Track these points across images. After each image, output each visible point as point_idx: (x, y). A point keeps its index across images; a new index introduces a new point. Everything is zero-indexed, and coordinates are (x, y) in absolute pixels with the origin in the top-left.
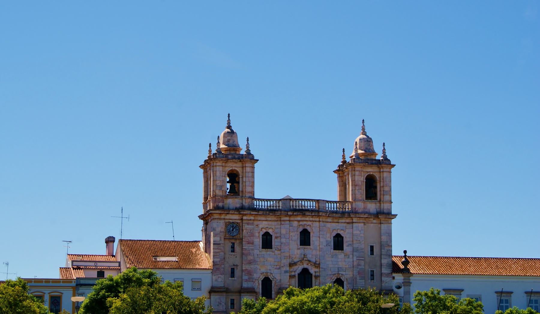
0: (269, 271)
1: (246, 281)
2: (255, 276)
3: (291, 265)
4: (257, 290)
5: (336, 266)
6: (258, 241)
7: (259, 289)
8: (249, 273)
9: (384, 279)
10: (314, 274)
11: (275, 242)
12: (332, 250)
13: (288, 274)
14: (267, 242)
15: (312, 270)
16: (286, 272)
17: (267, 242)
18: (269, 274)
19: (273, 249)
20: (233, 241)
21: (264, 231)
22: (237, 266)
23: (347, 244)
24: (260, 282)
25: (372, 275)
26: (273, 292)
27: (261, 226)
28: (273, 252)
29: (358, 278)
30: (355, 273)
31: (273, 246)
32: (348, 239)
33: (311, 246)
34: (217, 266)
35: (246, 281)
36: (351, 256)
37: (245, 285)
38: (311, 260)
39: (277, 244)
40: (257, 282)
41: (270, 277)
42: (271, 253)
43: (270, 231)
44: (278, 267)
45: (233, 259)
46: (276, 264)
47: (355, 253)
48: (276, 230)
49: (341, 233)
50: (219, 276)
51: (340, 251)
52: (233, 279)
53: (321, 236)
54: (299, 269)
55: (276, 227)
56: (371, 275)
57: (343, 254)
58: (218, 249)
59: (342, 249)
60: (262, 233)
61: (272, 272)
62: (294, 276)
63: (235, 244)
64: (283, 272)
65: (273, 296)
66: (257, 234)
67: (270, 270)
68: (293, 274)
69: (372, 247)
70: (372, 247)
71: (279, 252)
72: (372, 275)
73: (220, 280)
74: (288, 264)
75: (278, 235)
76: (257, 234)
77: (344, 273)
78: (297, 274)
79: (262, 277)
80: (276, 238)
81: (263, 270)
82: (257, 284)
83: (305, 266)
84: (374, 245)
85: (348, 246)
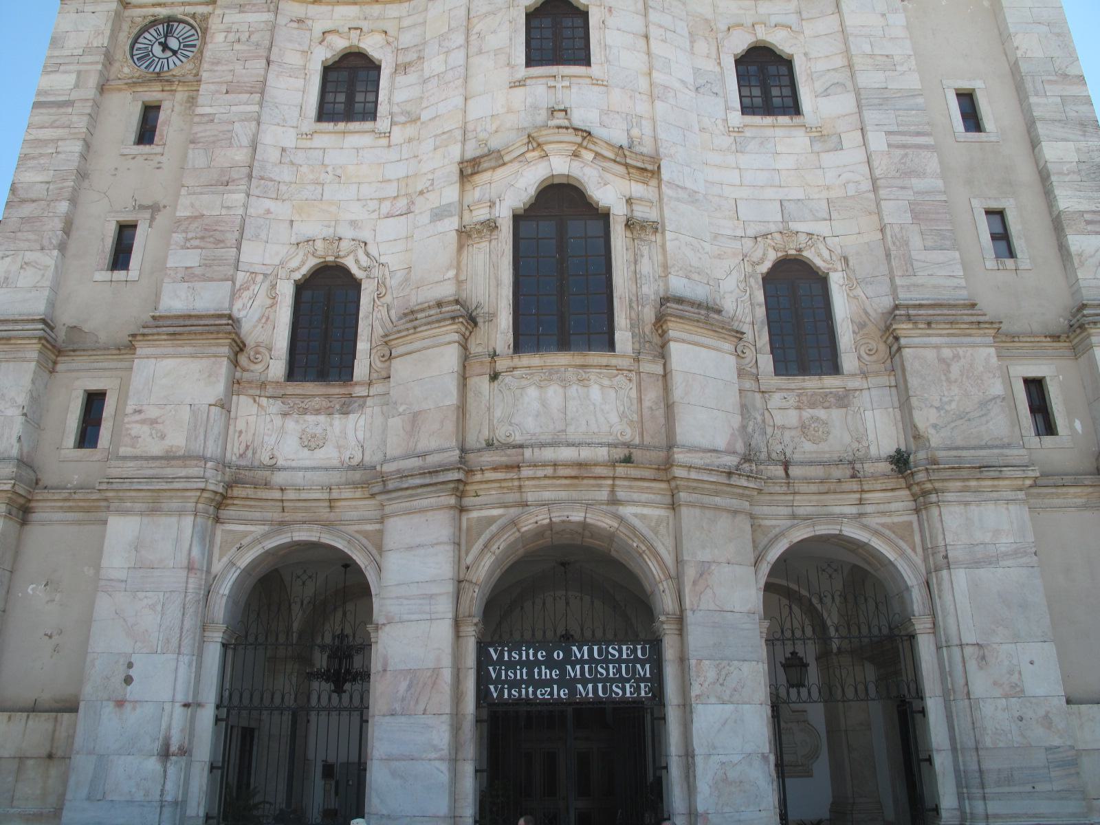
0: (347, 232)
1: (188, 276)
2: (252, 254)
3: (469, 170)
4: (251, 330)
5: (770, 193)
6: (300, 89)
7: (272, 325)
8: (220, 241)
9: (1076, 242)
10: (619, 211)
11: (392, 91)
12: (736, 117)
13: (452, 224)
14: (349, 87)
15: (608, 191)
16: (438, 215)
17: (349, 87)
18: (345, 245)
19: (382, 123)
20: (152, 94)
21: (340, 44)
22: (155, 209)
23: (819, 86)
24: (286, 292)
25: (1002, 237)
26: (362, 346)
27: (318, 28)
28: (381, 134)
29: (916, 242)
30: (895, 212)
31: (382, 109)
32: (820, 66)
33: (595, 69)
34: (26, 210)
35: (188, 276)
36: (852, 138)
37: (176, 300)
38: (597, 131)
39: (399, 96)
40: (261, 289)
41: (350, 263)
42: (367, 140)
43: (372, 46)
44: (402, 203)
45: (125, 179)
46: (391, 190)
47: (871, 116)
48: (407, 39)
49: (781, 41)
50: (30, 256)
51: (783, 120)
52: (120, 275)
53: (654, 32)
54: (517, 186)
55: (405, 23)
56: (994, 237)
57: (800, 133)
58: (52, 126)
59: (793, 107)
60: (322, 55)
61: (365, 235)
62: (491, 226)
63: (166, 106)
64: (426, 218)
65: (361, 369)
66: (293, 59)
67: (353, 223)
68: (482, 214)
69: (967, 100)
70: (967, 100)
71: (410, 130)
72: (1002, 237)
73: (28, 278)
74: (455, 170)
75: (412, 56)
76: (293, 59)
77: (822, 228)
78: (504, 215)
79: (303, 265)
80: (402, 68)
81: (312, 227)
82: (262, 299)
83: (560, 165)
84: (977, 85)
85: (826, 93)
